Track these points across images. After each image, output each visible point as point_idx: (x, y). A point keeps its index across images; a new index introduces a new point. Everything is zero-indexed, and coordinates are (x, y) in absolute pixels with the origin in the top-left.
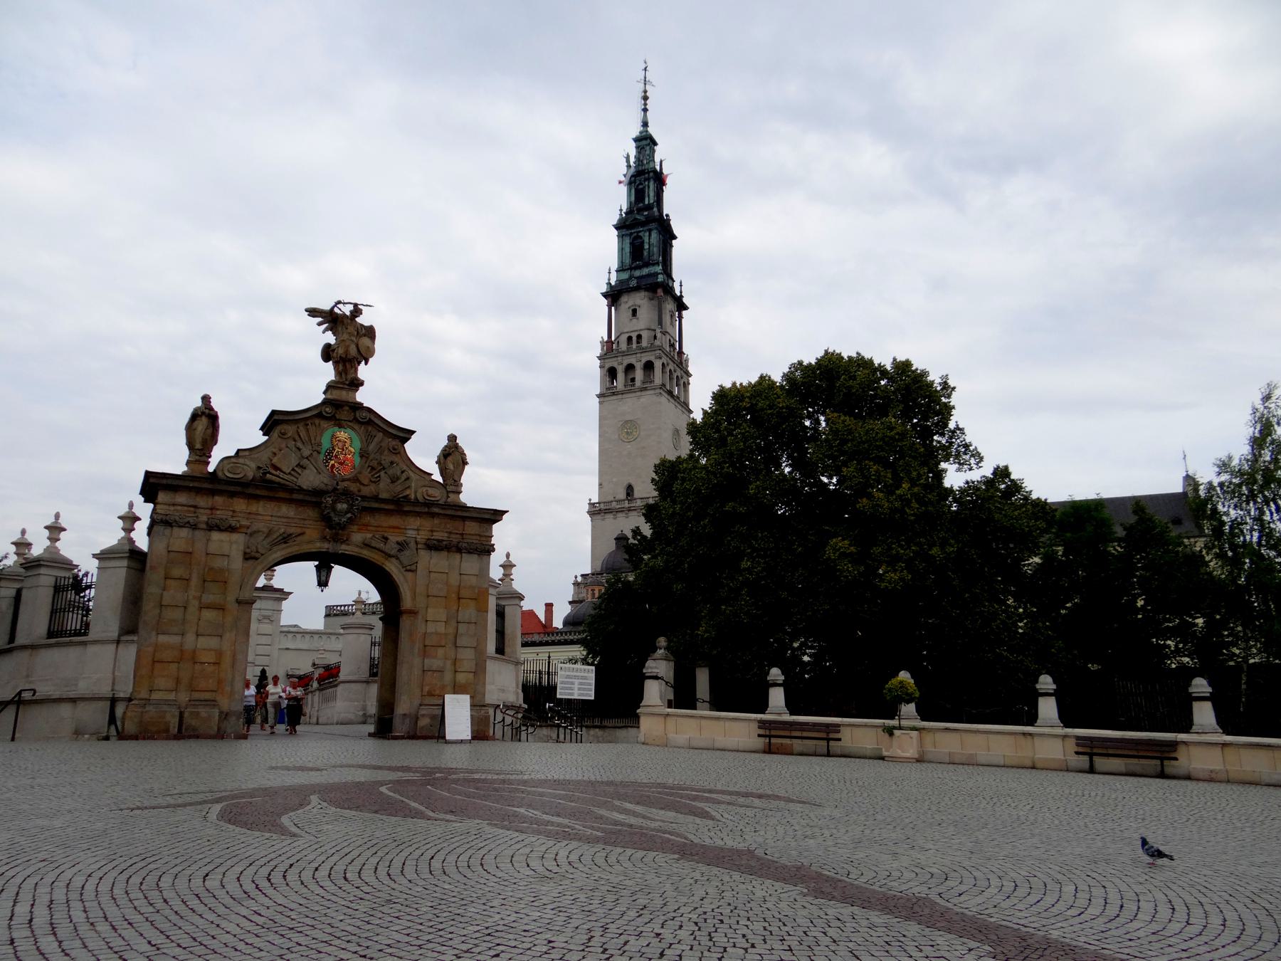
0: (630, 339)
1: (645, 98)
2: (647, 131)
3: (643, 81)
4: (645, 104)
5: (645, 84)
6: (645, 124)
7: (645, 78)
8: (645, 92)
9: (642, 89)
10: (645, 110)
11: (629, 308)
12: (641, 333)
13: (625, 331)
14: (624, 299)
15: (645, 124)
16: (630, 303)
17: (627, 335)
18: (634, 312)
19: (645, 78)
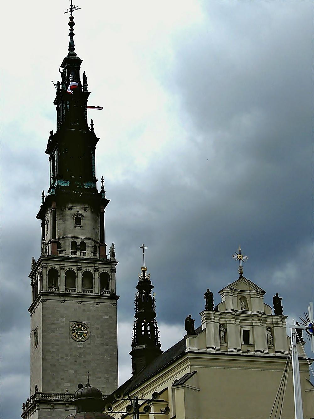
0: (74, 244)
1: (72, 24)
2: (75, 55)
3: (69, 10)
4: (72, 30)
5: (72, 11)
6: (72, 47)
7: (72, 5)
8: (72, 18)
9: (70, 16)
10: (72, 35)
13: (69, 235)
15: (72, 47)
16: (74, 211)
17: (71, 240)
18: (78, 220)
19: (72, 5)
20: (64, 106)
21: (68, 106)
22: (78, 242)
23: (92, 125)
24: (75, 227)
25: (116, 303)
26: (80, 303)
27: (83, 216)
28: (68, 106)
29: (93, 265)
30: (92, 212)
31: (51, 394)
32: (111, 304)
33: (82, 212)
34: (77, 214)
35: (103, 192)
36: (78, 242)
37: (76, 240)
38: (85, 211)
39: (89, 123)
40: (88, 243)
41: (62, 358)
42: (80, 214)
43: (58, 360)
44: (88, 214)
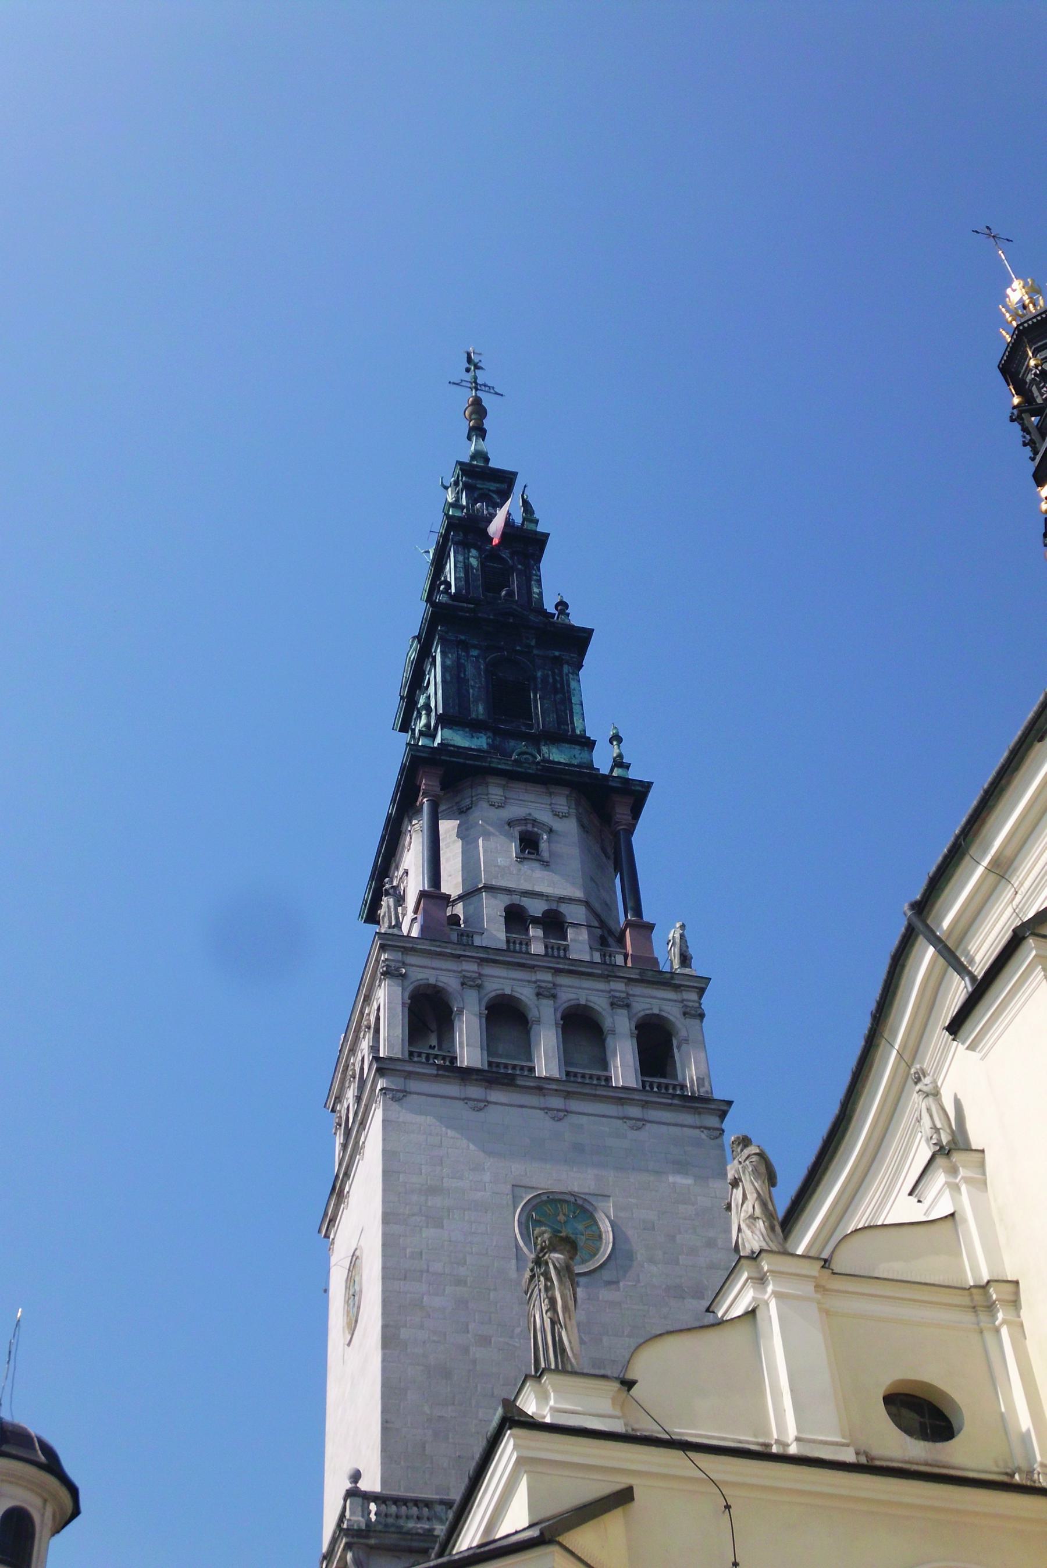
1: (478, 410)
10: (478, 431)
11: (510, 823)
12: (564, 908)
14: (496, 792)
16: (515, 811)
20: (461, 558)
21: (474, 562)
22: (536, 908)
23: (562, 606)
24: (521, 859)
25: (717, 1125)
26: (559, 1115)
27: (551, 831)
28: (474, 562)
29: (601, 986)
30: (582, 826)
31: (428, 1504)
32: (697, 1131)
33: (544, 816)
34: (525, 820)
35: (619, 762)
36: (536, 908)
37: (526, 902)
38: (556, 814)
39: (549, 606)
40: (575, 914)
41: (485, 1341)
42: (535, 822)
43: (466, 1350)
44: (569, 828)
